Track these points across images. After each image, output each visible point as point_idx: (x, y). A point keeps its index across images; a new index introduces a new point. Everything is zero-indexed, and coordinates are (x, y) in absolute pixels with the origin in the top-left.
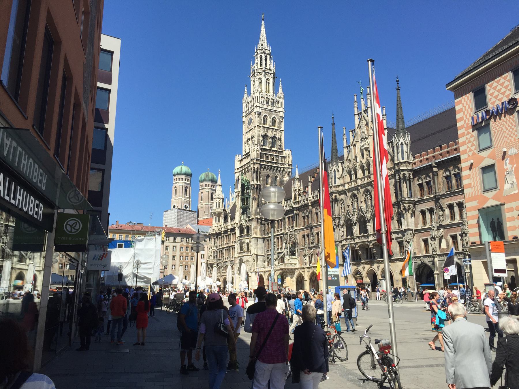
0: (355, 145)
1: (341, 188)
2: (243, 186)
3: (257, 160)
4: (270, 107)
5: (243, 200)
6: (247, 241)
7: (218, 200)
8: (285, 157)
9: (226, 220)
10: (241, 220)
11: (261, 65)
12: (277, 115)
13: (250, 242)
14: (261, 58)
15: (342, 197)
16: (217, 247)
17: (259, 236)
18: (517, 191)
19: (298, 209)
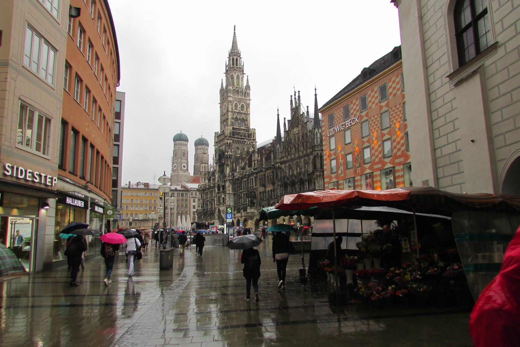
0: (290, 131)
1: (282, 160)
2: (219, 155)
3: (230, 137)
4: (240, 97)
5: (220, 166)
6: (223, 196)
7: (204, 165)
8: (251, 134)
9: (209, 180)
10: (218, 181)
11: (233, 64)
12: (245, 103)
13: (225, 196)
14: (233, 59)
15: (283, 166)
16: (203, 200)
17: (231, 192)
18: (343, 175)
19: (257, 173)
